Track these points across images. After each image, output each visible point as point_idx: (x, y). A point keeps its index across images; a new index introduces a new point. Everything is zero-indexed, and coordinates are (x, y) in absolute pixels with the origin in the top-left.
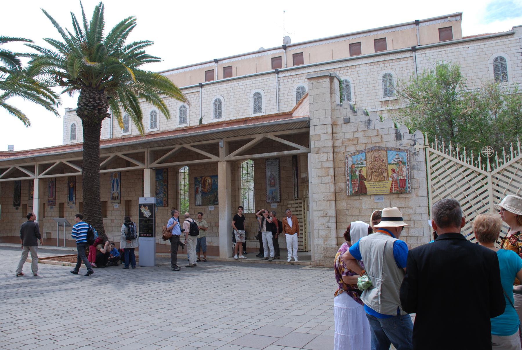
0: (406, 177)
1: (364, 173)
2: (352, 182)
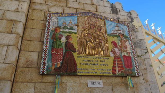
0: (130, 54)
1: (74, 41)
2: (53, 51)
